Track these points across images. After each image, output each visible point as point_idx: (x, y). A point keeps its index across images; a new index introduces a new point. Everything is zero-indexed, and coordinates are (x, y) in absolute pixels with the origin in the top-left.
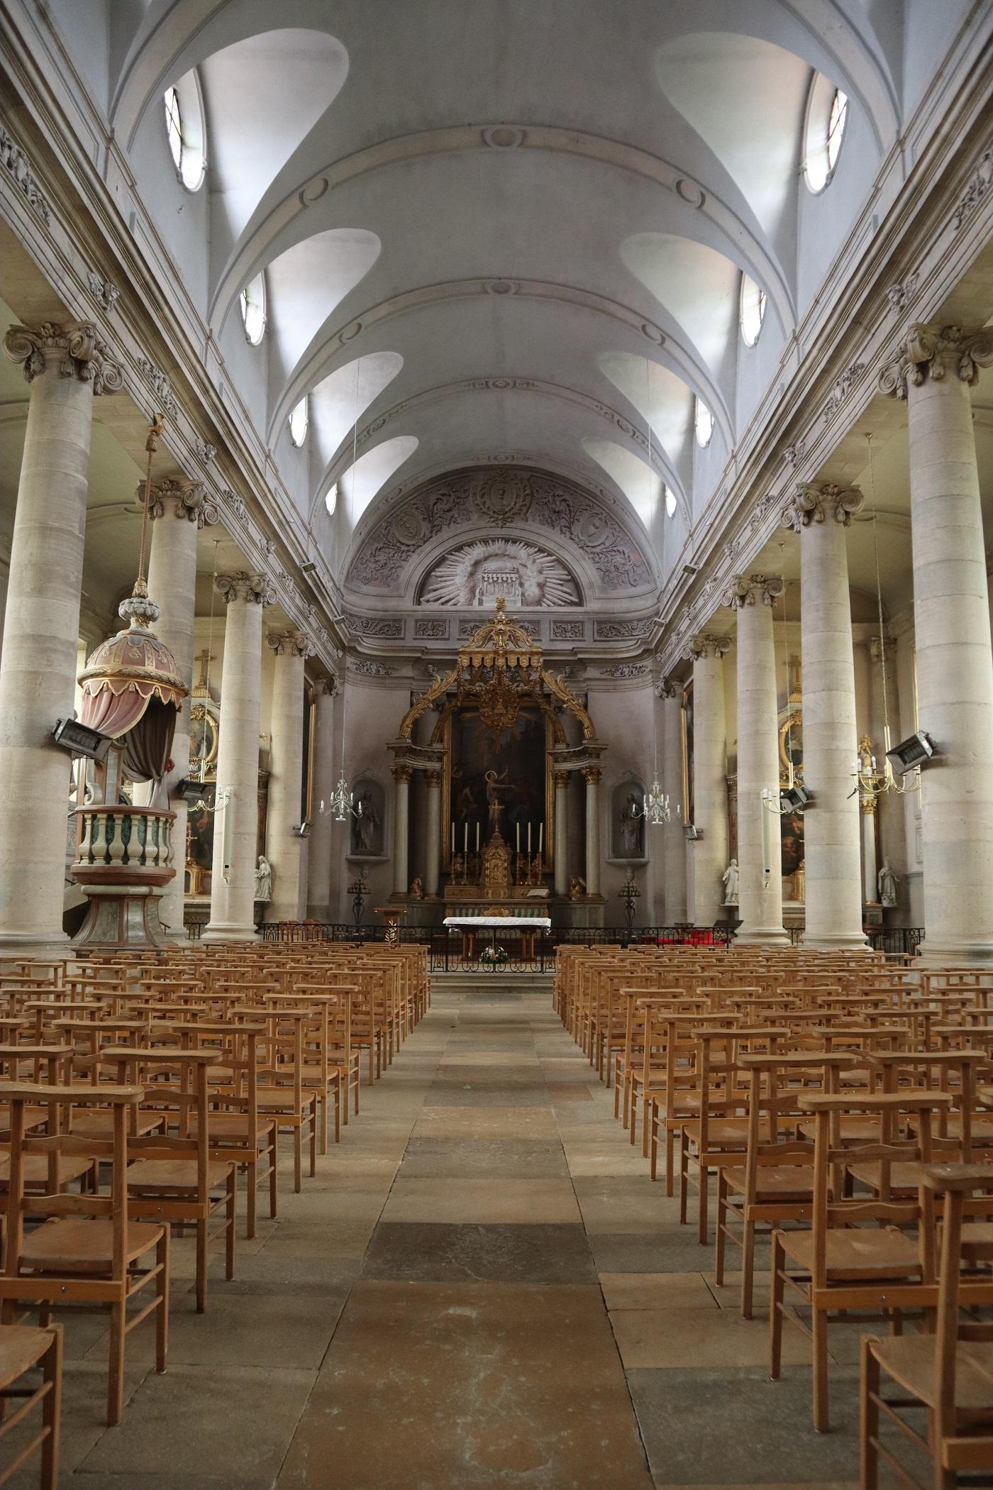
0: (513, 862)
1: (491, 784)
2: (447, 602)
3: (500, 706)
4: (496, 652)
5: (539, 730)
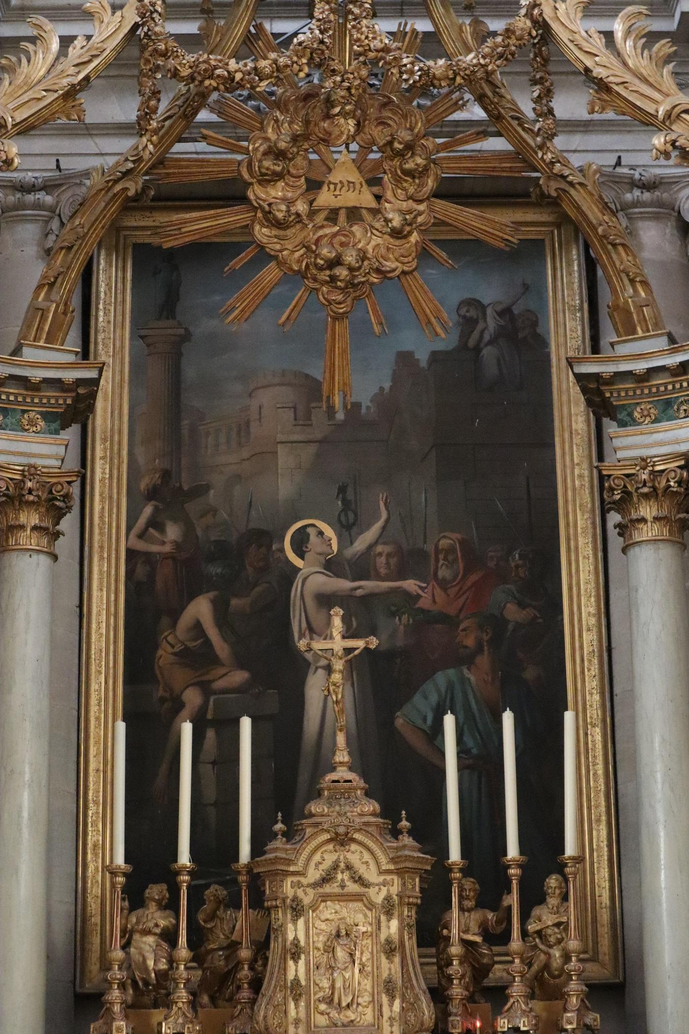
0: (429, 931)
1: (312, 578)
5: (524, 337)
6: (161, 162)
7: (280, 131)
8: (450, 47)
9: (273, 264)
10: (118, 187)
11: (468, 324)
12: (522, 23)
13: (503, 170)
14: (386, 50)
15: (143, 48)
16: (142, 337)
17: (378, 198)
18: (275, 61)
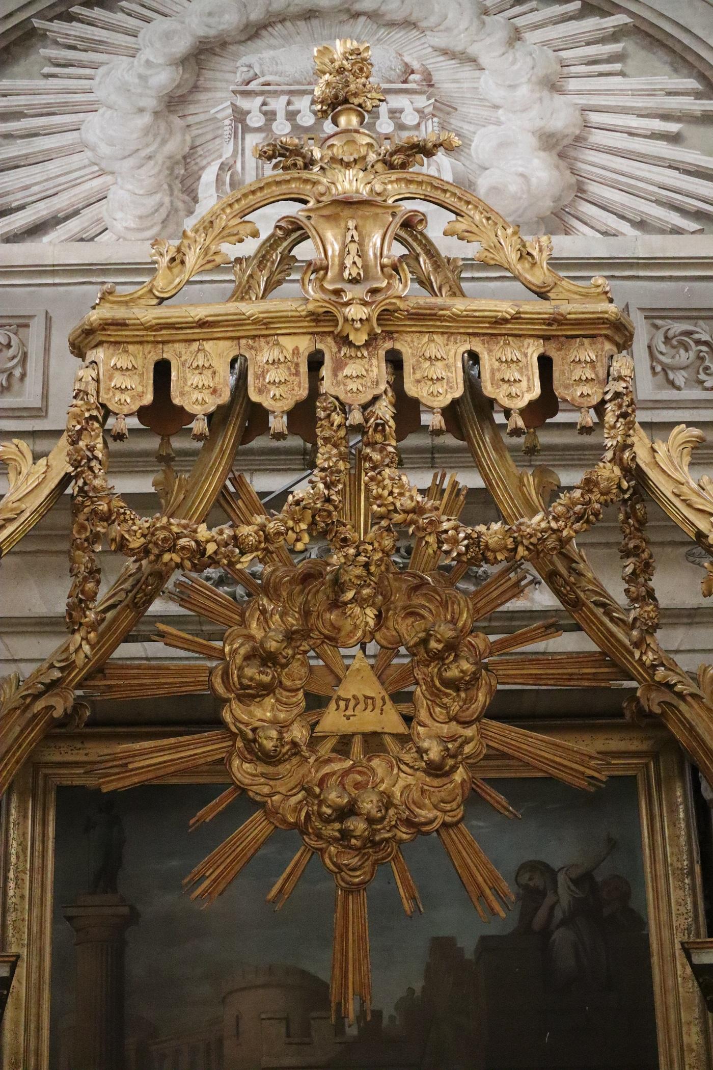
2: (36, 230)
3: (360, 682)
4: (322, 321)
6: (100, 669)
7: (268, 627)
8: (506, 507)
9: (258, 814)
10: (39, 705)
11: (531, 897)
12: (608, 472)
13: (583, 677)
14: (418, 510)
15: (76, 510)
16: (70, 919)
17: (408, 719)
18: (263, 527)
